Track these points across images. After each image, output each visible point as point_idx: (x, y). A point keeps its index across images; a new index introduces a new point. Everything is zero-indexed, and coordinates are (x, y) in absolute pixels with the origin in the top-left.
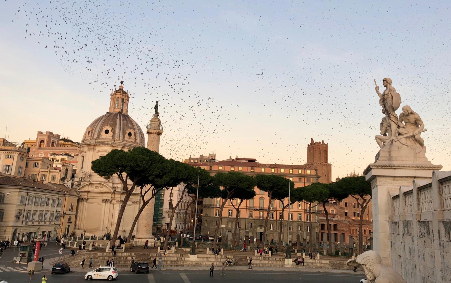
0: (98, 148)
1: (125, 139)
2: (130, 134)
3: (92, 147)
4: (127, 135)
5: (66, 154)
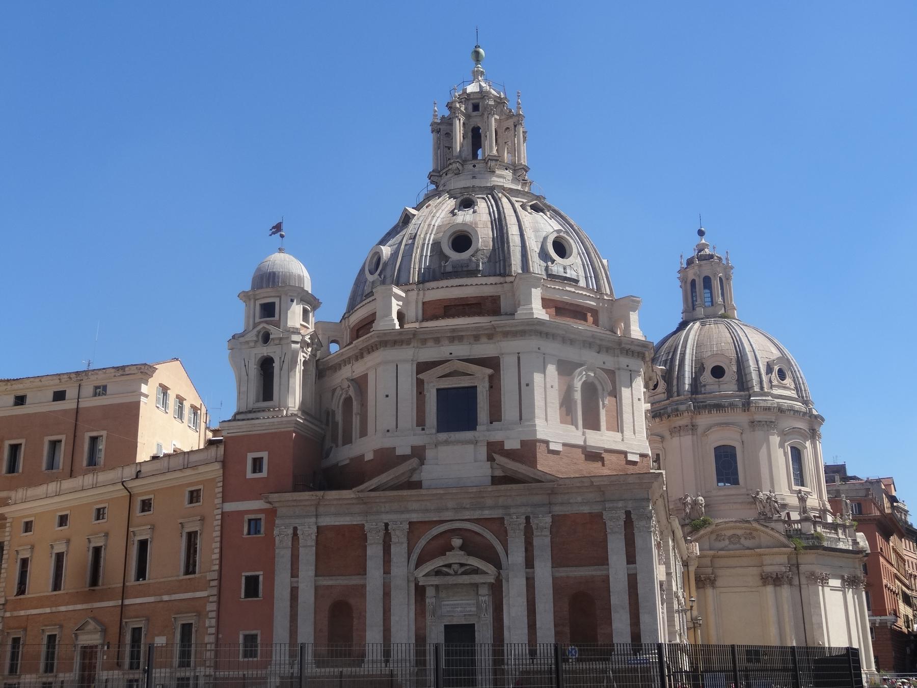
2: (782, 375)
4: (774, 376)
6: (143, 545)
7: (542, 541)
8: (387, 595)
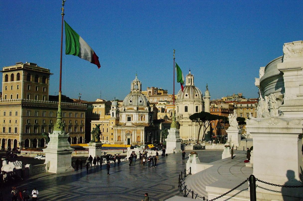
0: (183, 103)
1: (195, 98)
2: (196, 95)
3: (181, 103)
4: (195, 96)
5: (166, 101)
6: (103, 128)
7: (135, 132)
8: (123, 136)
